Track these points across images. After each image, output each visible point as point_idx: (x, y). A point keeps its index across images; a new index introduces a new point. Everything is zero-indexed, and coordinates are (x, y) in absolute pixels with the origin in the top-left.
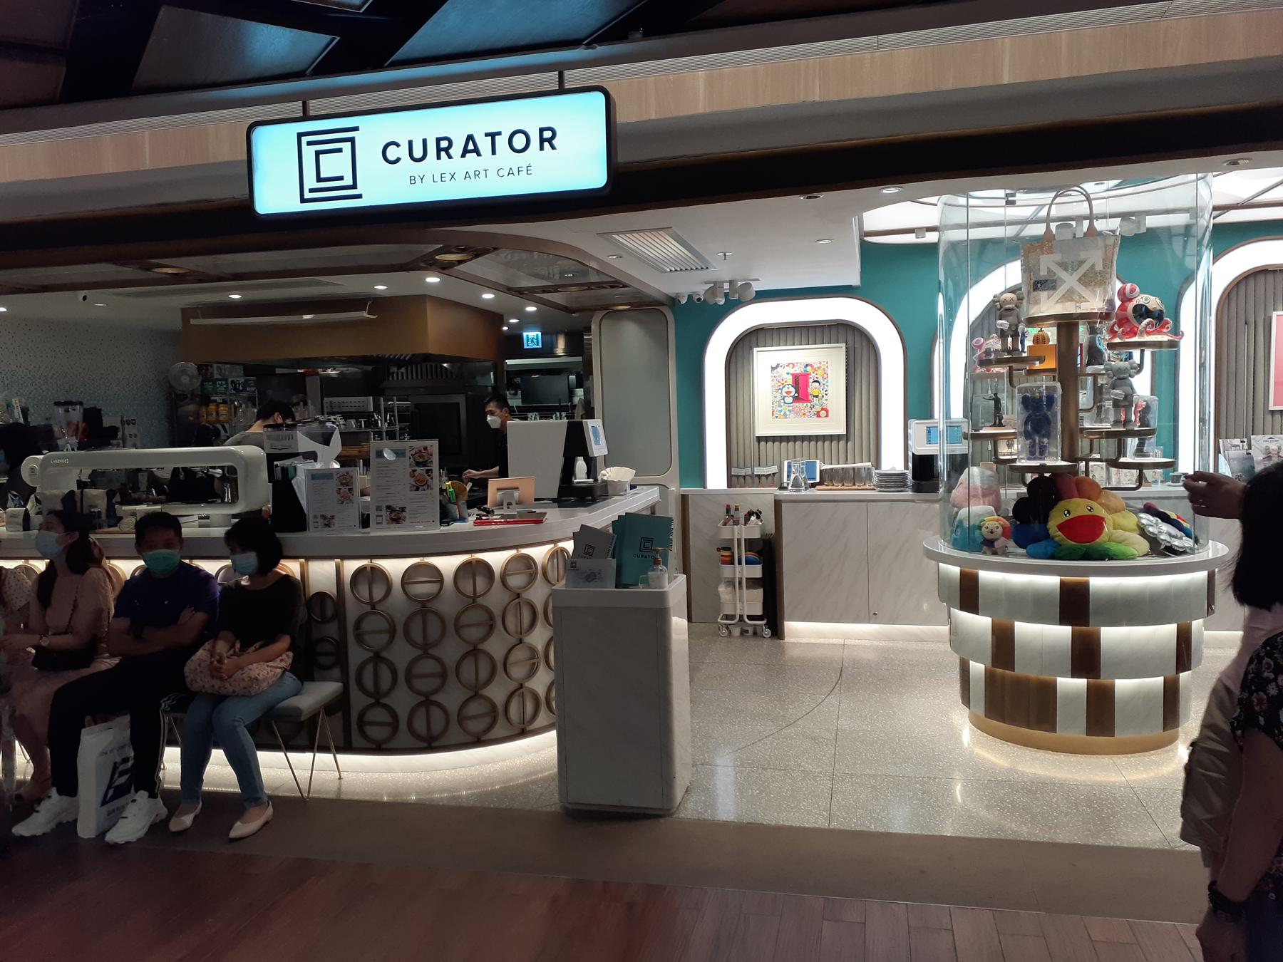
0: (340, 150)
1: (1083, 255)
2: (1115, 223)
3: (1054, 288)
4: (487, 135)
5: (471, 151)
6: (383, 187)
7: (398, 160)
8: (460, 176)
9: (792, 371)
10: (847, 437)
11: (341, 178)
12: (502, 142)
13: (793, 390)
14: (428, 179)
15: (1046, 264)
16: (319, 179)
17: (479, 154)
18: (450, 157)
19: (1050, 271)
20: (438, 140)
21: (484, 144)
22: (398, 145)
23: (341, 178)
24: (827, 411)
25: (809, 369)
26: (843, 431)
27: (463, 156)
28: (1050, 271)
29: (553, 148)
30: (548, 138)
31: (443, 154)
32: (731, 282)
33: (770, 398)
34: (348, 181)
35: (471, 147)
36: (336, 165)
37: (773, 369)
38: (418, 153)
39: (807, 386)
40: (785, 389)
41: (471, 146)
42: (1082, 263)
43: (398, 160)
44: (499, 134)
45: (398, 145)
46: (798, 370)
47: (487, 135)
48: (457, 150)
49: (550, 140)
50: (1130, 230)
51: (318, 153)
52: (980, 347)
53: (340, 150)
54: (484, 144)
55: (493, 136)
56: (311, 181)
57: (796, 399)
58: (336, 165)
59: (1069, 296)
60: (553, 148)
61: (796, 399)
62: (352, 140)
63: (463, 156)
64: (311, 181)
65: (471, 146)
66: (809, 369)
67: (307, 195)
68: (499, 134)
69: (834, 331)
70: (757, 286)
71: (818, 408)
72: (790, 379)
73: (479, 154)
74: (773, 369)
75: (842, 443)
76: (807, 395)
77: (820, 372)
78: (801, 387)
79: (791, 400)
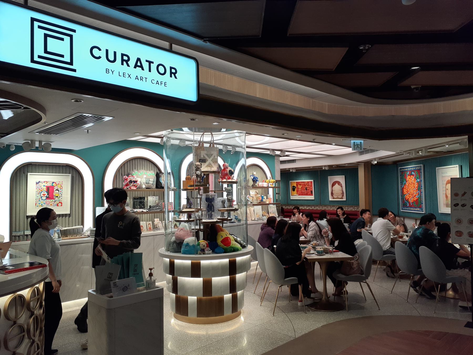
0: (62, 39)
1: (212, 153)
2: (177, 142)
3: (205, 162)
4: (147, 61)
5: (139, 66)
6: (87, 69)
7: (99, 58)
8: (133, 77)
9: (46, 185)
10: (69, 215)
11: (62, 56)
12: (154, 67)
13: (46, 193)
14: (116, 73)
15: (203, 154)
16: (46, 52)
17: (143, 69)
18: (128, 65)
19: (204, 156)
20: (123, 55)
21: (146, 65)
22: (100, 50)
23: (62, 56)
24: (61, 203)
25: (54, 184)
26: (68, 212)
27: (135, 67)
28: (204, 156)
29: (176, 78)
30: (173, 72)
31: (125, 63)
32: (40, 142)
33: (35, 197)
34: (67, 59)
35: (138, 64)
36: (59, 46)
37: (37, 183)
38: (111, 58)
39: (53, 192)
40: (43, 193)
41: (139, 64)
42: (212, 155)
43: (99, 58)
44: (153, 63)
45: (100, 50)
46: (49, 185)
47: (147, 61)
48: (132, 62)
49: (175, 74)
50: (182, 144)
51: (46, 36)
52: (126, 179)
53: (62, 39)
54: (146, 65)
55: (150, 63)
56: (39, 50)
57: (47, 198)
58: (59, 46)
59: (209, 165)
60: (176, 78)
61: (47, 198)
62: (71, 36)
63: (135, 67)
64: (39, 50)
65: (139, 64)
66: (54, 184)
67: (36, 59)
68: (153, 63)
69: (64, 168)
70: (54, 146)
71: (57, 202)
72: (45, 189)
73: (143, 69)
74: (37, 183)
75: (67, 217)
76: (53, 196)
77: (59, 186)
78: (50, 192)
79: (45, 198)
